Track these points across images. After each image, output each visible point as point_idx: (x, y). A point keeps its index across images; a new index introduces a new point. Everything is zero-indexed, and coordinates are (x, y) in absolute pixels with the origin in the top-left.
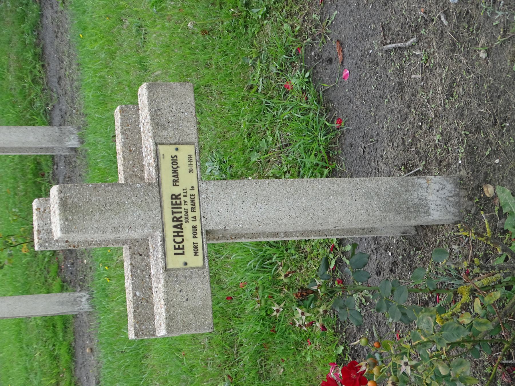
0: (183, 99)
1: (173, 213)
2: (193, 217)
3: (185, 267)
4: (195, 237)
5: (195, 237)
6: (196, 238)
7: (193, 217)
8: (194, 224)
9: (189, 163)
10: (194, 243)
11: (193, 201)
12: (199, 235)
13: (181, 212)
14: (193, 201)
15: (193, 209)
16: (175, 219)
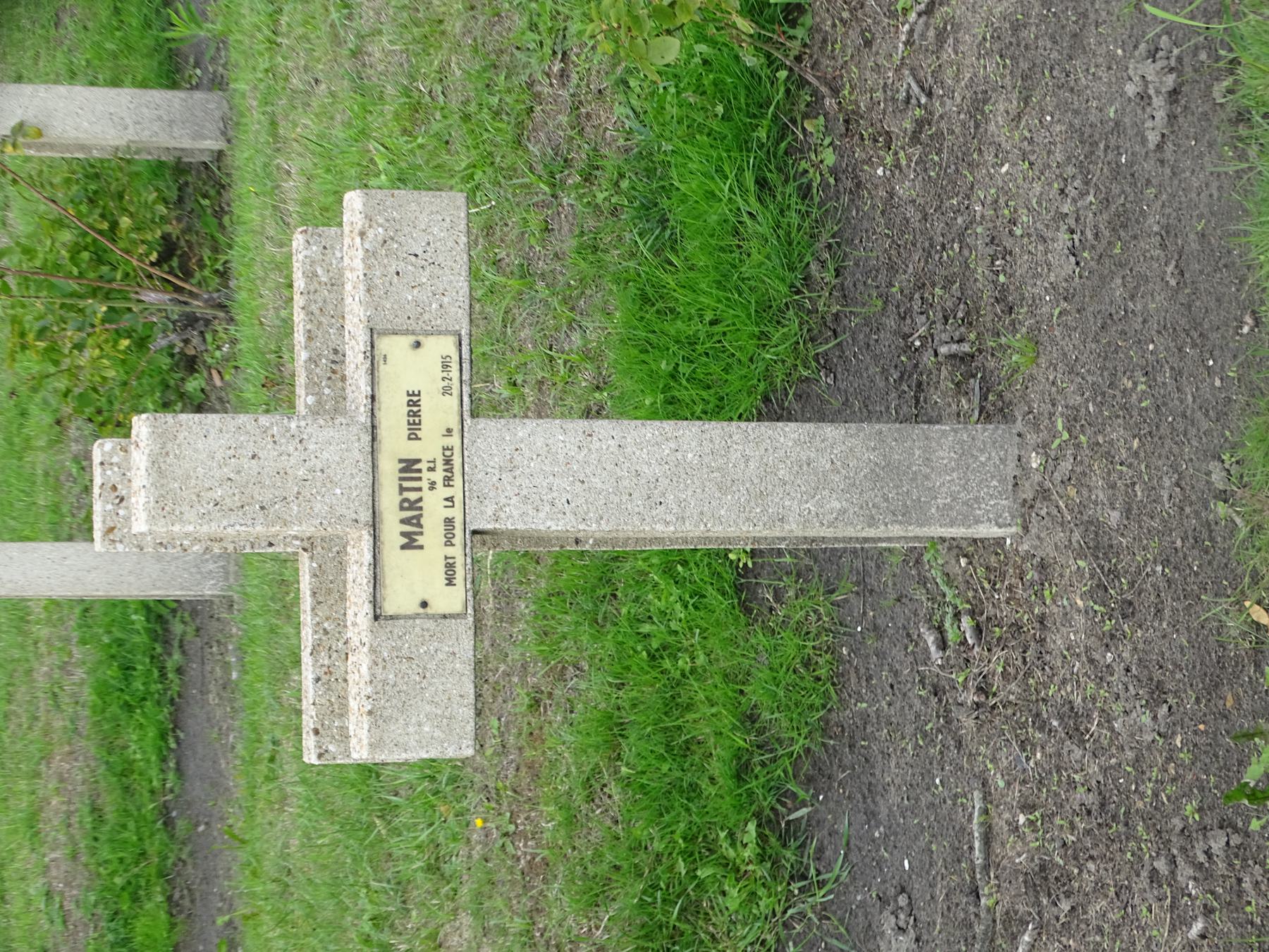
0: (439, 224)
1: (402, 489)
2: (446, 499)
3: (421, 611)
4: (449, 543)
5: (449, 543)
6: (453, 545)
7: (446, 499)
8: (449, 513)
9: (445, 374)
10: (446, 558)
11: (448, 461)
12: (458, 540)
13: (420, 489)
14: (448, 461)
15: (448, 481)
16: (406, 505)
